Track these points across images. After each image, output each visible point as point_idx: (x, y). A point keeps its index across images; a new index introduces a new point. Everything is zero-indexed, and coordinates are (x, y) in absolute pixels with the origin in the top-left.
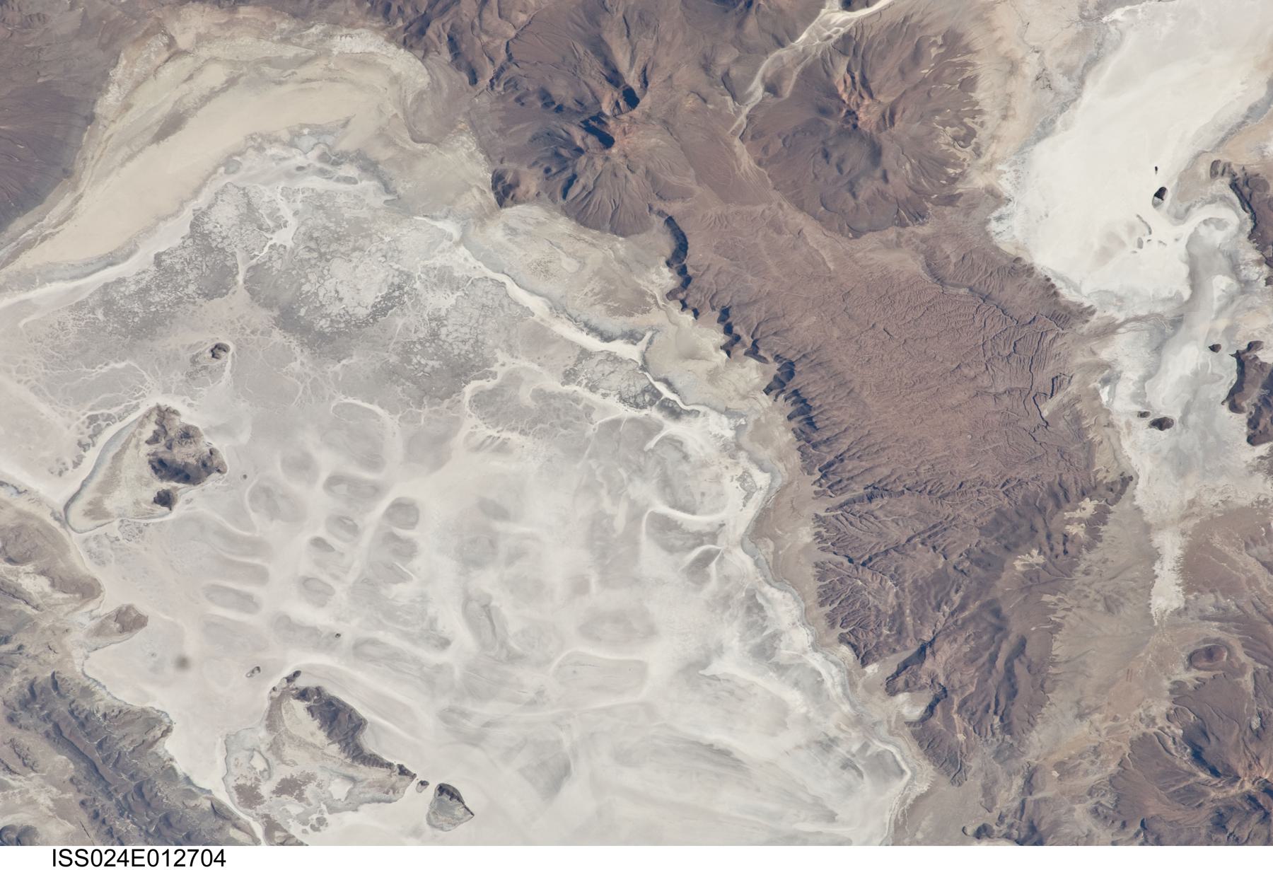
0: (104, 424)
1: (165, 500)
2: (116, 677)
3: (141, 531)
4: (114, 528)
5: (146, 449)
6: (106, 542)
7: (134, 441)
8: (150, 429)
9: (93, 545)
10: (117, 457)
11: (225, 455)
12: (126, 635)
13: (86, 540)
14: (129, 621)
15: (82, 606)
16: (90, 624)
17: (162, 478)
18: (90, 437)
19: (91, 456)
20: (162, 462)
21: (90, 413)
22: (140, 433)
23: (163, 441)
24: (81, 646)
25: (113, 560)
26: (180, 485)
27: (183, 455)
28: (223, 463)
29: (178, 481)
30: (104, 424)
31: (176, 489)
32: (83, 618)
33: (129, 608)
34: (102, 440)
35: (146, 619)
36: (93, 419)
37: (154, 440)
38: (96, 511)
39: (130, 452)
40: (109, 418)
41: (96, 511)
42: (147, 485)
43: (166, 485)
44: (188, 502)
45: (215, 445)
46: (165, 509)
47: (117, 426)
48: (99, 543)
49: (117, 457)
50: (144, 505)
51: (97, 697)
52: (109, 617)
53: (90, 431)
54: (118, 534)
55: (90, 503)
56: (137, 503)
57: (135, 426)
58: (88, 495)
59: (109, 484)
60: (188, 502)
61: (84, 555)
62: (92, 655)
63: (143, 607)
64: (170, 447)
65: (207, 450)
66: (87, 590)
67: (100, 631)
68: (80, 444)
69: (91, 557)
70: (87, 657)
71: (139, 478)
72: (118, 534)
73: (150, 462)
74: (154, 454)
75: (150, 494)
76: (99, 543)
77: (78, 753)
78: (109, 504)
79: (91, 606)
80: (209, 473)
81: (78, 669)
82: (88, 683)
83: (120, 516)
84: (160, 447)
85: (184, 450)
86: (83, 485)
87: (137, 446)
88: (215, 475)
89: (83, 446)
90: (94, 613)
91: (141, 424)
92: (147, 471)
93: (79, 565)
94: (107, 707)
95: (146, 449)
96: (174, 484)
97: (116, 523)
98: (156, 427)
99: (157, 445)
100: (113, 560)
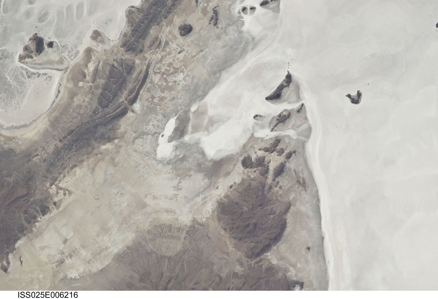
0: (30, 73)
1: (51, 45)
2: (117, 30)
3: (64, 46)
4: (65, 54)
5: (35, 58)
6: (70, 54)
7: (33, 62)
8: (27, 60)
9: (72, 57)
10: (39, 64)
11: (31, 36)
12: (102, 34)
13: (72, 60)
14: (96, 35)
15: (94, 50)
16: (101, 45)
17: (43, 49)
18: (35, 75)
19: (41, 71)
20: (37, 51)
21: (27, 78)
22: (30, 62)
23: (31, 54)
24: (109, 44)
25: (76, 49)
26: (45, 43)
27: (33, 47)
28: (34, 35)
29: (43, 44)
30: (30, 73)
31: (46, 44)
32: (99, 48)
33: (91, 37)
34: (35, 71)
35: (94, 31)
36: (29, 77)
37: (31, 57)
38: (61, 61)
39: (37, 62)
40: (27, 73)
41: (61, 61)
42: (47, 52)
43: (45, 46)
44: (49, 38)
45: (28, 40)
46: (54, 43)
47: (30, 69)
48: (72, 55)
49: (39, 64)
50: (55, 49)
51: (126, 32)
52: (97, 41)
53: (34, 76)
54: (67, 53)
55: (58, 64)
56: (54, 52)
57: (28, 64)
58: (57, 66)
59: (50, 62)
60: (49, 38)
61: (77, 58)
62: (111, 40)
63: (90, 33)
64: (32, 52)
65: (30, 42)
66: (89, 52)
67: (102, 42)
68: (38, 76)
69: (77, 56)
70: (113, 41)
71: (45, 55)
72: (67, 53)
73: (39, 55)
74: (36, 55)
75: (51, 49)
76: (72, 55)
77: (148, 27)
78: (57, 59)
79: (94, 48)
80: (38, 37)
81: (118, 41)
82: (121, 36)
83: (60, 54)
84: (33, 55)
85: (32, 48)
86: (53, 69)
87: (35, 61)
88: (38, 35)
89: (39, 75)
90: (96, 46)
91: (27, 63)
92: (42, 54)
93: (81, 58)
94: (129, 27)
95: (35, 58)
96: (45, 45)
97: (63, 54)
98: (27, 59)
99: (33, 56)
100: (76, 49)
